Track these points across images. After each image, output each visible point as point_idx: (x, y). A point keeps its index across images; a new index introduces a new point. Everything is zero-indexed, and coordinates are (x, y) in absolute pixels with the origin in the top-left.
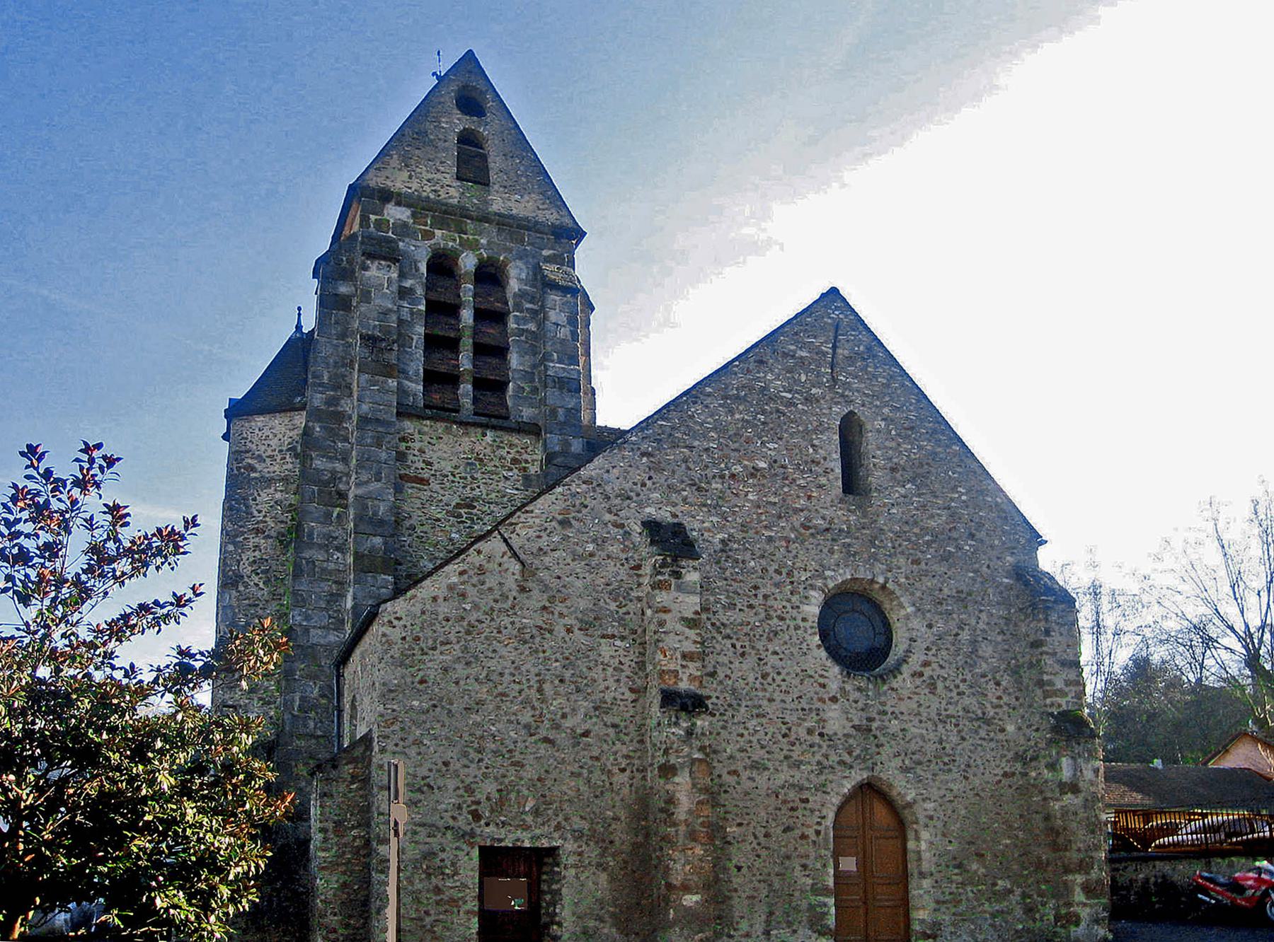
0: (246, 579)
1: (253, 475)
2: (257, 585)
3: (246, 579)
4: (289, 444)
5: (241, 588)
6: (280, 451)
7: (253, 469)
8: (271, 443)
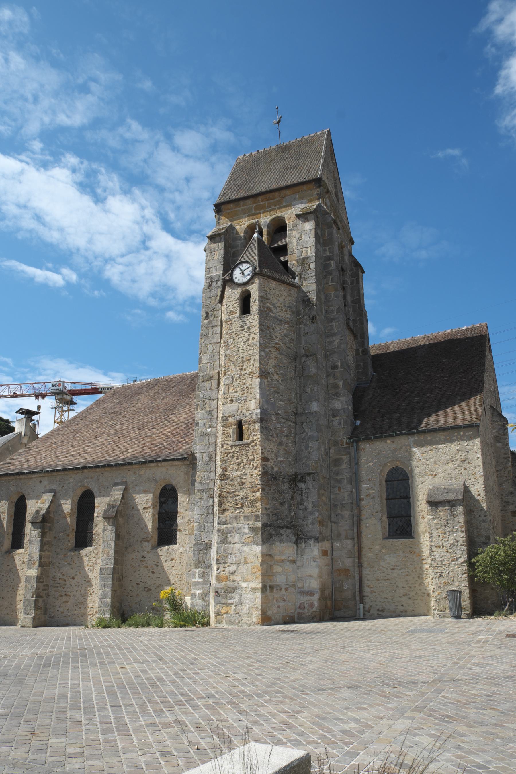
0: (271, 375)
1: (272, 314)
2: (278, 381)
3: (271, 375)
4: (289, 303)
5: (269, 379)
6: (285, 306)
7: (270, 310)
8: (280, 299)
